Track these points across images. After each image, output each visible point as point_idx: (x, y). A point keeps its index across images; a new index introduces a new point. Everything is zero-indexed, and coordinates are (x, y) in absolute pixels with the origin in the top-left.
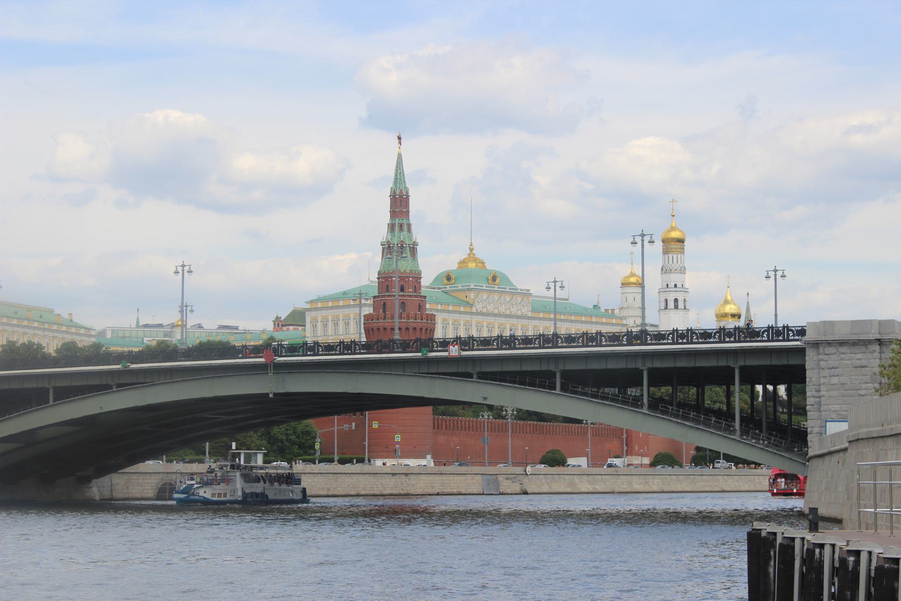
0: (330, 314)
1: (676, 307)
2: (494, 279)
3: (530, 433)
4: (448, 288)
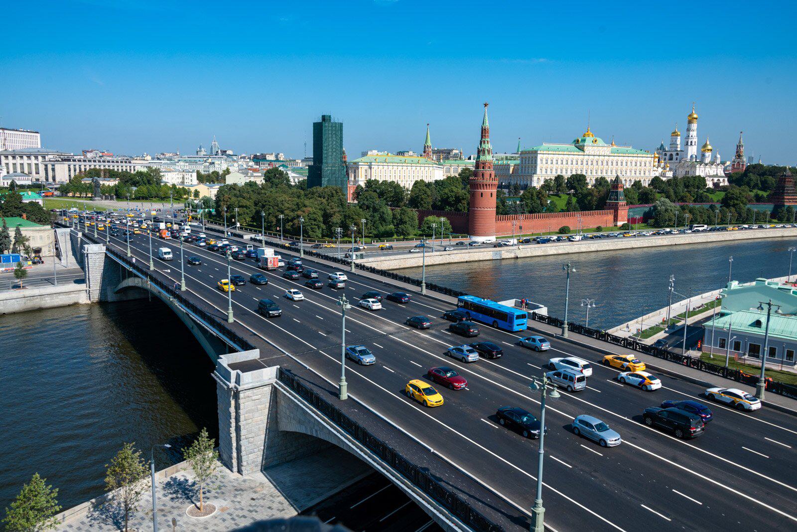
1: (691, 144)
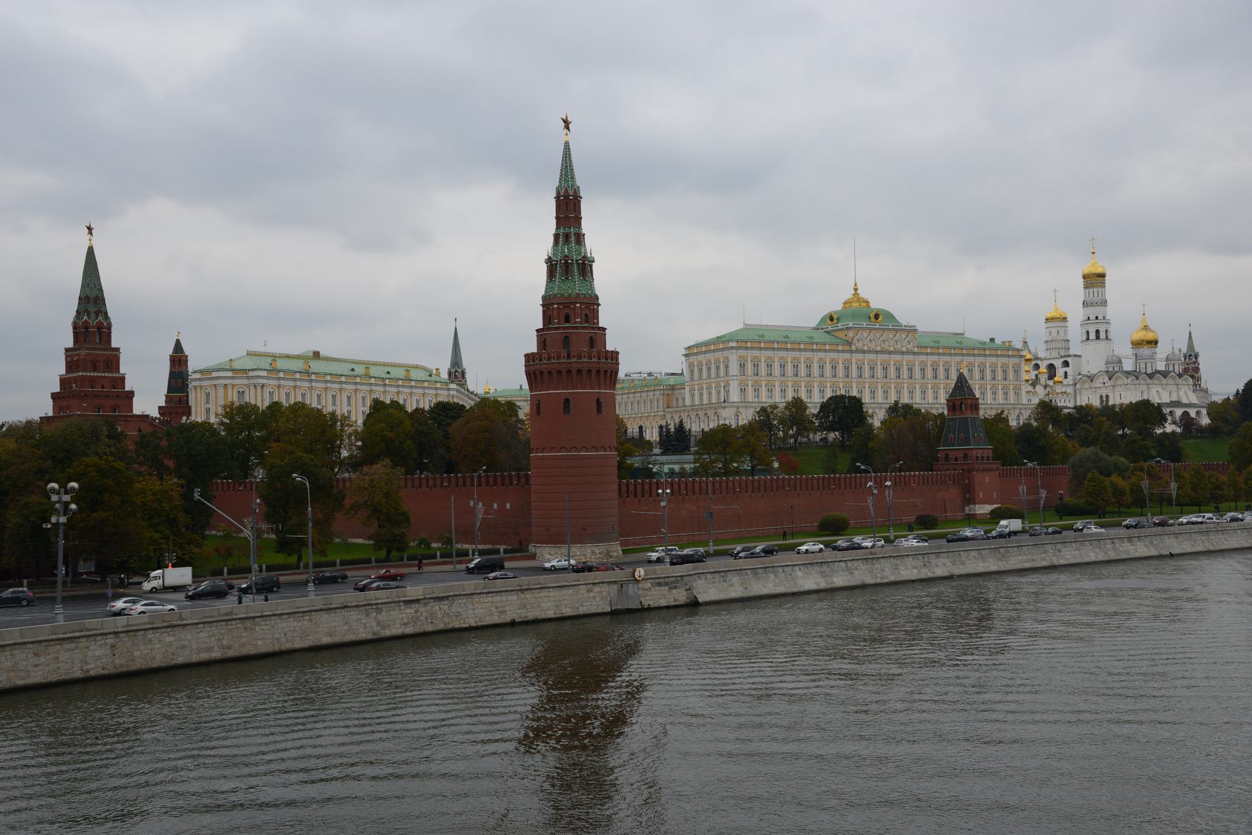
0: (700, 357)
1: (1098, 337)
2: (877, 316)
3: (818, 489)
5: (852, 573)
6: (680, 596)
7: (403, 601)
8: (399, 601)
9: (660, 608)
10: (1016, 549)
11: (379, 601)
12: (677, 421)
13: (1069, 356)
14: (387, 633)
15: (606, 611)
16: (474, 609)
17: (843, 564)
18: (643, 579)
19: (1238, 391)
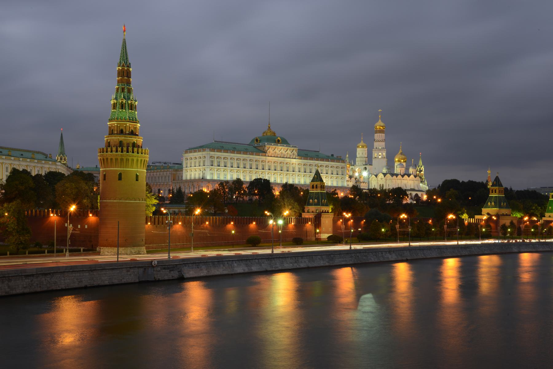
4: (256, 144)
5: (261, 265)
6: (175, 274)
7: (25, 276)
8: (22, 275)
9: (164, 280)
10: (338, 256)
11: (10, 275)
12: (178, 187)
13: (367, 165)
14: (14, 292)
15: (136, 281)
16: (65, 280)
17: (257, 261)
18: (156, 266)
19: (439, 185)
